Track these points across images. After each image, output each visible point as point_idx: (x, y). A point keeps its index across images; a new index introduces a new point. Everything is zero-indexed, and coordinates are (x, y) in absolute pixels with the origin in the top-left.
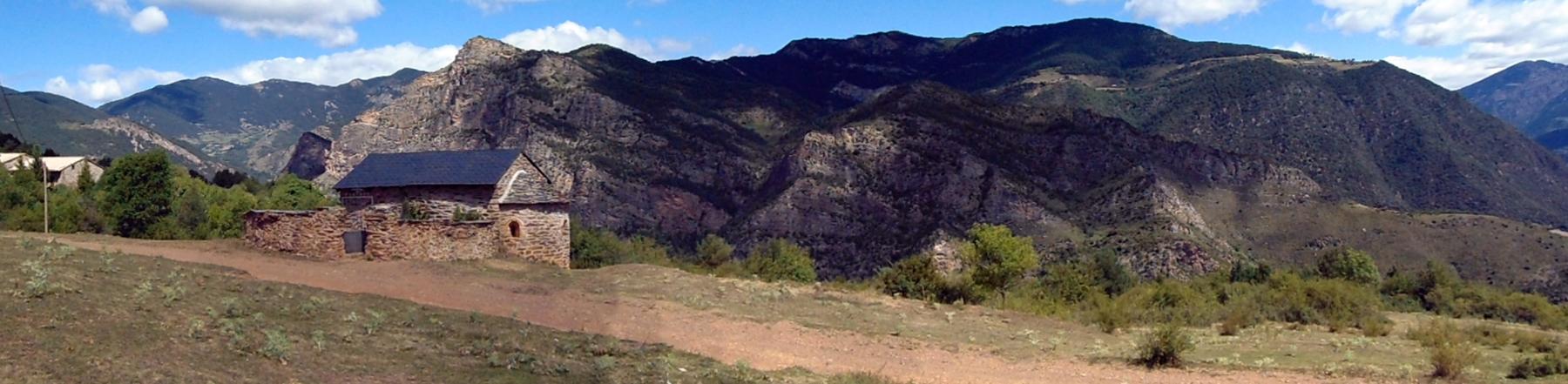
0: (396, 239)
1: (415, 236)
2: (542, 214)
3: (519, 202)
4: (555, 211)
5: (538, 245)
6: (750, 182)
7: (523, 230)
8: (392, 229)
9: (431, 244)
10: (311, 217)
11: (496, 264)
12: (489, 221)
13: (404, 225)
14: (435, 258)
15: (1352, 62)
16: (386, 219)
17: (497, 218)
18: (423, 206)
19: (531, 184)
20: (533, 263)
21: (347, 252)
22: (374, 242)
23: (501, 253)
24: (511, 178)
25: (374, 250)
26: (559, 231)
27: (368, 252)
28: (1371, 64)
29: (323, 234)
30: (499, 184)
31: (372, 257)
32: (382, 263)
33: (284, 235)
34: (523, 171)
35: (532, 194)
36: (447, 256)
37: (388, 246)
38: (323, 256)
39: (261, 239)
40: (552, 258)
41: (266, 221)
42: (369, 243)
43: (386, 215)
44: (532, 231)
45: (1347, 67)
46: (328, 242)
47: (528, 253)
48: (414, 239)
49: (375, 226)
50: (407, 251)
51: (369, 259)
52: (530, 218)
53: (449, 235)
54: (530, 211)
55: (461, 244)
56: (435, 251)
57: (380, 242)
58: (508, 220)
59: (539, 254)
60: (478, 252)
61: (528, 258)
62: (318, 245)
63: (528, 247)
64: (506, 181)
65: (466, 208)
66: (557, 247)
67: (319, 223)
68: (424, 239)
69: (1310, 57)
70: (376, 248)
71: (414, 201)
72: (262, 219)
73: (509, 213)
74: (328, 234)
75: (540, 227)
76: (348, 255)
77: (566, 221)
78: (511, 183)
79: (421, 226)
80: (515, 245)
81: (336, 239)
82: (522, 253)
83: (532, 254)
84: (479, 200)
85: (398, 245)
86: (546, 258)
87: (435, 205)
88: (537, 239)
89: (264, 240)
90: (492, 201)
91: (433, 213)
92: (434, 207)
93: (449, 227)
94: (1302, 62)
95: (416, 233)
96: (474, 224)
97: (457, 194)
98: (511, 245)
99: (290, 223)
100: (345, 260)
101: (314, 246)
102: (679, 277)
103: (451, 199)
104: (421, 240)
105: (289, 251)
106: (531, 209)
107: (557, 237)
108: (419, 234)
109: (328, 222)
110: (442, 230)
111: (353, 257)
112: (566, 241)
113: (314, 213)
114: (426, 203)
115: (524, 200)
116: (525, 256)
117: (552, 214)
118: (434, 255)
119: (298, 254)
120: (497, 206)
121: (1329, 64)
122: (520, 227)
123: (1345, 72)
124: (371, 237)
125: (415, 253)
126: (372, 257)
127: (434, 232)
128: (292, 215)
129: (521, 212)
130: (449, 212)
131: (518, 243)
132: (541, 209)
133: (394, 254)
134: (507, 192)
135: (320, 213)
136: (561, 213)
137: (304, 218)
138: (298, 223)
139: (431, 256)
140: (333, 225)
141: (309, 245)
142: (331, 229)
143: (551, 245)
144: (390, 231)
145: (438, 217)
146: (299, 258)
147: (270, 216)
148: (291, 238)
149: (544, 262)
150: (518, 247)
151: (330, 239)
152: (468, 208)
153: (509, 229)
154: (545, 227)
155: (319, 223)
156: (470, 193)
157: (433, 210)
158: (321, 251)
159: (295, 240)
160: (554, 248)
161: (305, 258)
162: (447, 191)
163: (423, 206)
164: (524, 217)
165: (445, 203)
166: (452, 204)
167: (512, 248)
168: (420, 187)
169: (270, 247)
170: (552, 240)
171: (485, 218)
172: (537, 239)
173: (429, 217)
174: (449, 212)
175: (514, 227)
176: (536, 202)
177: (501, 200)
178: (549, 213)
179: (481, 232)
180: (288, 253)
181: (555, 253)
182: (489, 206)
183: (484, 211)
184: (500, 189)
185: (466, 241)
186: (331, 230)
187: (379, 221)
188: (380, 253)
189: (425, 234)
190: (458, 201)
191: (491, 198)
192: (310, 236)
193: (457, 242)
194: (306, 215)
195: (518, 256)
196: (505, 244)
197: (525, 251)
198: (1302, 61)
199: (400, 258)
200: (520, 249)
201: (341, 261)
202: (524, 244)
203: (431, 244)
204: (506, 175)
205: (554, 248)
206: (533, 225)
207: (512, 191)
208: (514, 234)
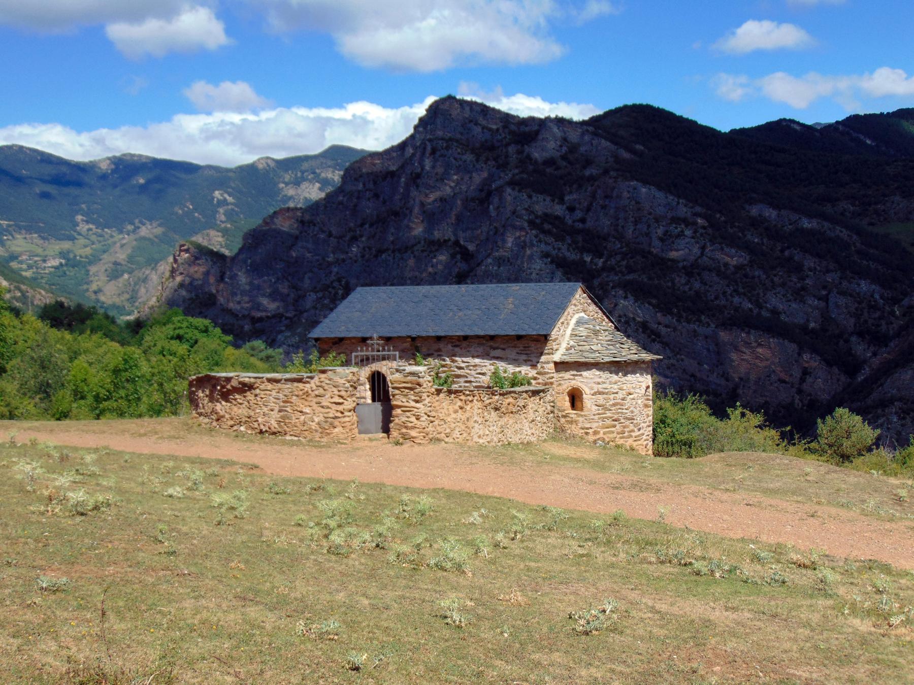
0: (433, 414)
1: (456, 412)
2: (615, 377)
3: (583, 360)
4: (634, 372)
5: (609, 422)
6: (883, 322)
7: (588, 400)
8: (428, 400)
9: (476, 422)
10: (308, 382)
11: (557, 449)
12: (541, 387)
13: (442, 395)
14: (481, 441)
16: (420, 385)
17: (552, 383)
18: (443, 366)
19: (596, 333)
20: (605, 448)
21: (360, 433)
22: (404, 419)
23: (559, 433)
24: (568, 324)
25: (404, 430)
26: (639, 402)
27: (394, 433)
29: (328, 408)
30: (554, 334)
31: (401, 440)
32: (417, 449)
33: (265, 409)
34: (582, 314)
35: (599, 347)
36: (495, 439)
37: (424, 424)
38: (325, 440)
39: (227, 416)
40: (630, 441)
41: (235, 390)
42: (397, 420)
43: (421, 380)
44: (601, 402)
46: (336, 417)
47: (595, 433)
48: (454, 416)
49: (406, 396)
50: (448, 431)
51: (397, 443)
52: (599, 383)
53: (496, 409)
54: (598, 373)
55: (511, 422)
56: (481, 433)
57: (413, 419)
58: (567, 386)
59: (611, 436)
60: (529, 432)
61: (595, 442)
62: (319, 424)
63: (594, 425)
64: (562, 329)
65: (508, 369)
66: (636, 425)
67: (321, 391)
68: (468, 414)
70: (406, 427)
71: (430, 359)
72: (229, 387)
73: (567, 375)
74: (335, 407)
75: (612, 396)
76: (363, 436)
77: (648, 387)
78: (569, 332)
79: (463, 397)
80: (576, 422)
81: (347, 414)
82: (587, 433)
83: (601, 435)
84: (524, 357)
85: (436, 423)
86: (621, 442)
87: (463, 365)
88: (609, 414)
89: (232, 419)
90: (543, 358)
91: (458, 376)
92: (460, 368)
93: (497, 397)
95: (457, 407)
96: (526, 392)
97: (494, 349)
98: (571, 422)
99: (274, 393)
100: (361, 444)
101: (314, 426)
102: (827, 473)
103: (485, 355)
104: (464, 418)
105: (274, 433)
106: (600, 369)
107: (636, 411)
108: (461, 408)
109: (335, 390)
110: (488, 402)
111: (370, 440)
112: (648, 416)
113: (312, 378)
114: (448, 362)
115: (591, 358)
116: (591, 438)
117: (630, 377)
118: (479, 437)
119: (288, 438)
120: (552, 365)
122: (584, 396)
124: (399, 411)
125: (456, 434)
126: (401, 440)
127: (479, 404)
128: (277, 381)
129: (585, 374)
130: (483, 374)
131: (581, 419)
132: (613, 369)
133: (431, 436)
134: (564, 345)
135: (323, 376)
136: (642, 374)
137: (296, 384)
138: (287, 392)
139: (476, 439)
140: (343, 393)
141: (304, 423)
142: (337, 400)
143: (628, 423)
144: (426, 402)
145: (466, 382)
146: (292, 444)
147: (240, 383)
148: (275, 415)
149: (618, 446)
150: (580, 425)
151: (339, 415)
152: (511, 369)
153: (567, 398)
154: (620, 395)
155: (321, 391)
156: (515, 347)
157: (459, 372)
158: (324, 432)
159: (281, 417)
160: (632, 427)
161: (297, 444)
162: (480, 344)
163: (443, 366)
164: (588, 381)
165: (477, 361)
166: (487, 362)
167: (574, 426)
168: (439, 338)
169: (242, 428)
170: (629, 415)
171: (533, 382)
172: (609, 414)
173: (453, 382)
174: (483, 374)
175: (575, 398)
176: (607, 359)
177: (557, 357)
178: (625, 375)
179: (533, 403)
180: (273, 437)
181: (633, 434)
182: (539, 366)
183: (532, 373)
184: (555, 340)
185: (517, 416)
186: (341, 401)
187: (411, 389)
188: (413, 433)
189: (468, 408)
190: (497, 358)
191: (542, 354)
192: (307, 410)
193: (505, 419)
194: (300, 380)
195: (582, 438)
196: (563, 420)
197: (590, 431)
199: (439, 440)
200: (582, 429)
201: (356, 445)
202: (591, 421)
203: (476, 422)
204: (561, 321)
205: (632, 427)
206: (603, 393)
207: (572, 343)
208: (573, 406)
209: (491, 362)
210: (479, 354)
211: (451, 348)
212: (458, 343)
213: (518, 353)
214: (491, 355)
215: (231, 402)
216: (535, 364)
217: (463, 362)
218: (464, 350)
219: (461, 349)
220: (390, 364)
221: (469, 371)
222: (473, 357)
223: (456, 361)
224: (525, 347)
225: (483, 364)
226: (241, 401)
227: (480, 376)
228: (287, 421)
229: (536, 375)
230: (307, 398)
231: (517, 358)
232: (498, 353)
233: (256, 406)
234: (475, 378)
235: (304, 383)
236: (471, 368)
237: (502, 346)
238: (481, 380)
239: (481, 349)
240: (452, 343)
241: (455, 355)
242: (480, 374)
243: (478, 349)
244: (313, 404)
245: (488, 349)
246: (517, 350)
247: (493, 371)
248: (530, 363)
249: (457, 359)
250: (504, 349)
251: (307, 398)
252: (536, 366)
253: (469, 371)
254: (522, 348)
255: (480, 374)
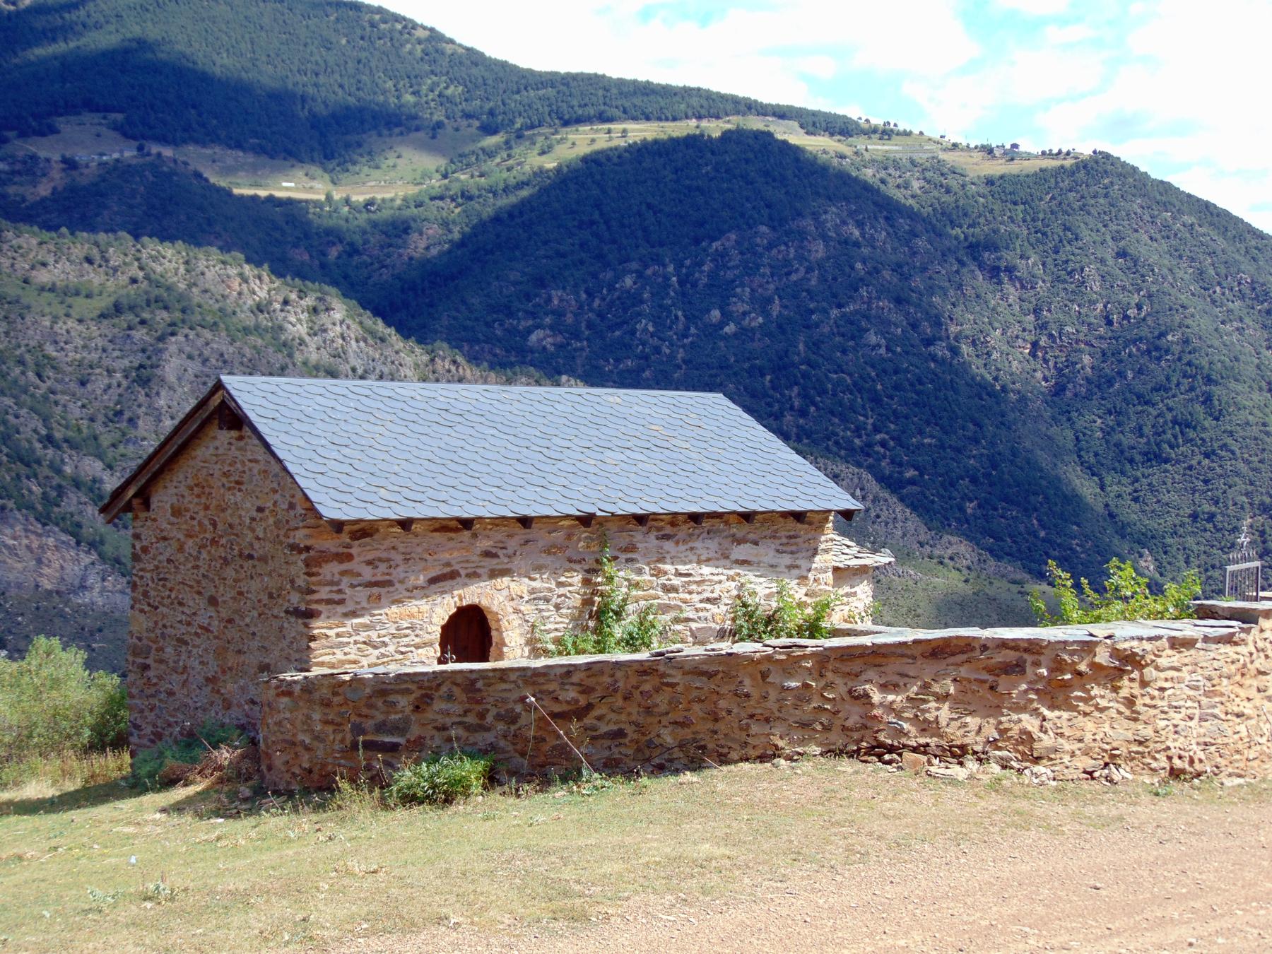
15: (1012, 153)
28: (1068, 163)
45: (997, 168)
69: (886, 133)
84: (787, 560)
87: (677, 581)
92: (668, 589)
94: (861, 147)
97: (740, 542)
103: (723, 557)
120: (830, 574)
121: (942, 156)
123: (990, 182)
128: (1189, 643)
165: (706, 570)
182: (811, 576)
190: (743, 563)
191: (815, 552)
198: (860, 143)
209: (731, 572)
210: (712, 555)
211: (656, 542)
212: (668, 530)
213: (778, 551)
214: (733, 557)
215: (1074, 708)
216: (805, 573)
217: (679, 574)
218: (682, 547)
219: (677, 543)
220: (513, 585)
221: (687, 596)
222: (699, 562)
223: (666, 573)
224: (790, 537)
225: (716, 578)
226: (1103, 703)
227: (708, 606)
228: (1219, 741)
229: (805, 599)
230: (1243, 681)
231: (773, 562)
232: (740, 552)
233: (1152, 712)
234: (697, 610)
235: (1236, 644)
236: (694, 587)
237: (751, 536)
238: (708, 615)
239: (713, 544)
240: (659, 529)
241: (662, 560)
242: (708, 600)
243: (709, 543)
244: (1253, 693)
245: (726, 543)
246: (774, 544)
247: (735, 593)
248: (795, 572)
249: (668, 567)
250: (756, 543)
251: (1243, 681)
252: (806, 578)
253: (687, 596)
254: (784, 540)
255: (708, 600)
